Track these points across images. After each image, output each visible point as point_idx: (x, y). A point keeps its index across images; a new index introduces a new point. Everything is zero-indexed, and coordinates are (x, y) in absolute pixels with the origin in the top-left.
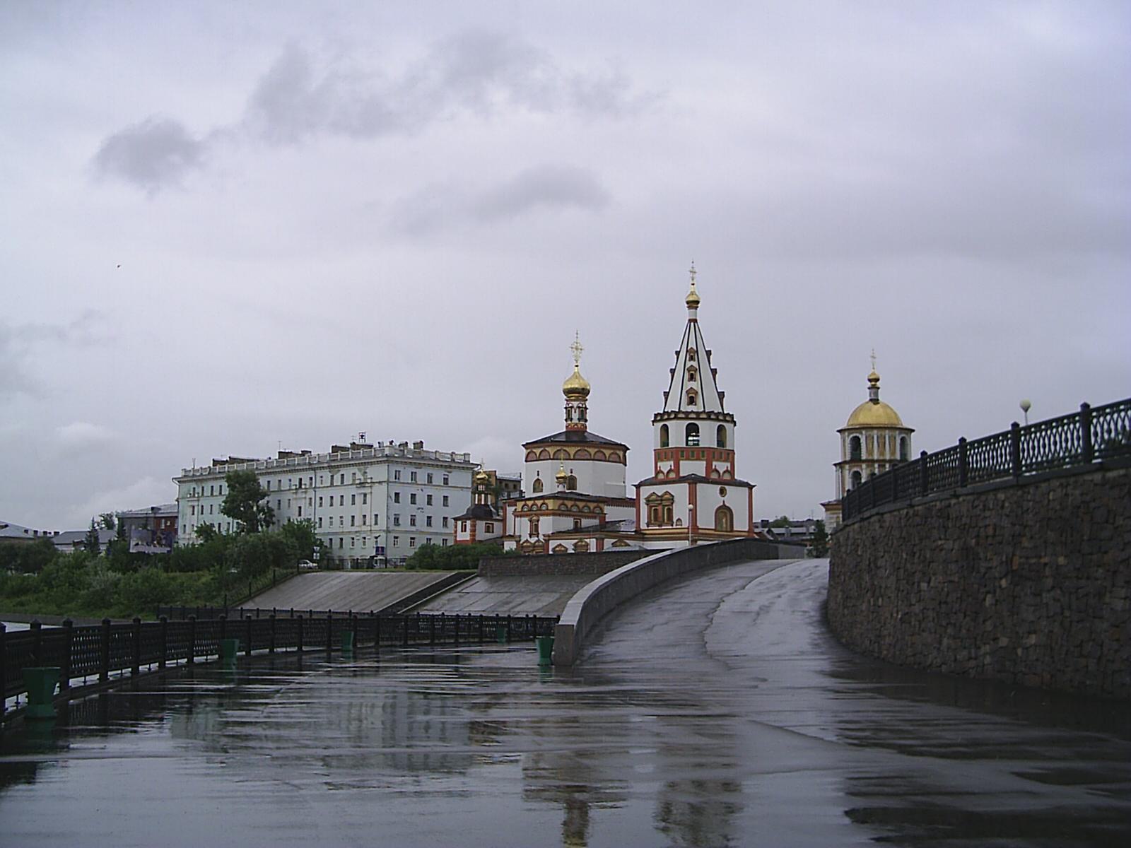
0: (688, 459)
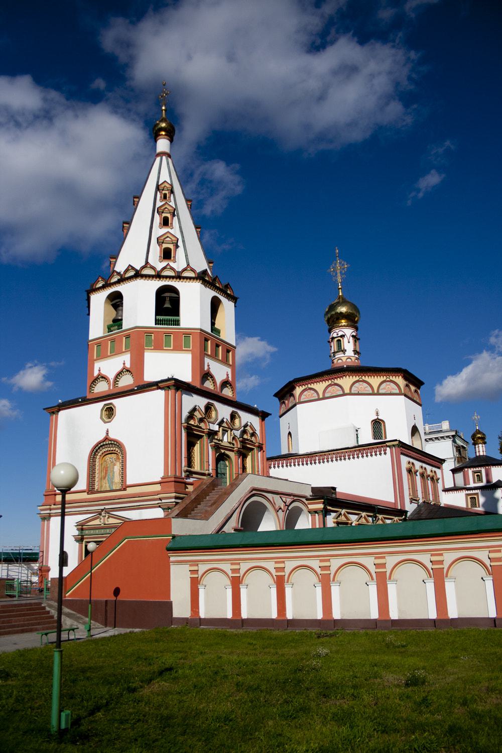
0: (158, 347)
